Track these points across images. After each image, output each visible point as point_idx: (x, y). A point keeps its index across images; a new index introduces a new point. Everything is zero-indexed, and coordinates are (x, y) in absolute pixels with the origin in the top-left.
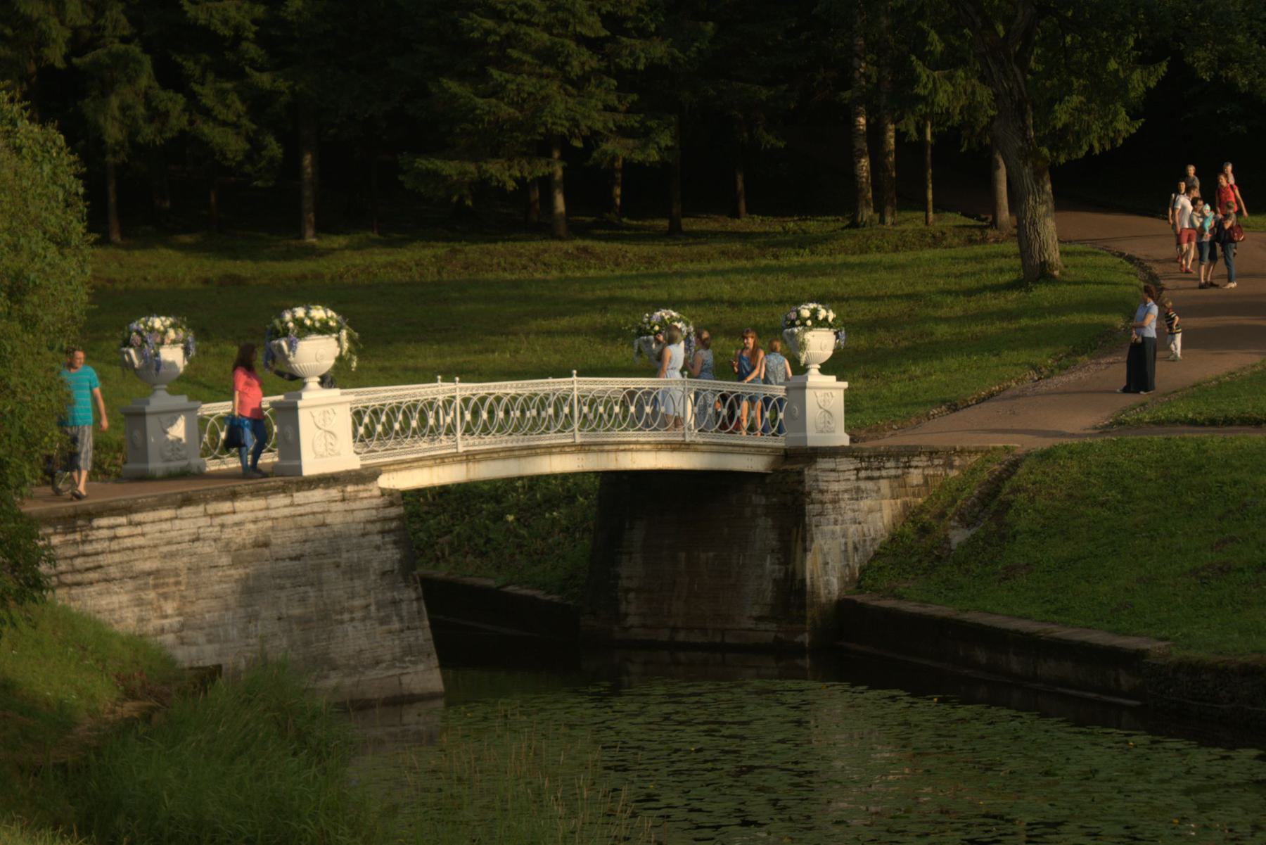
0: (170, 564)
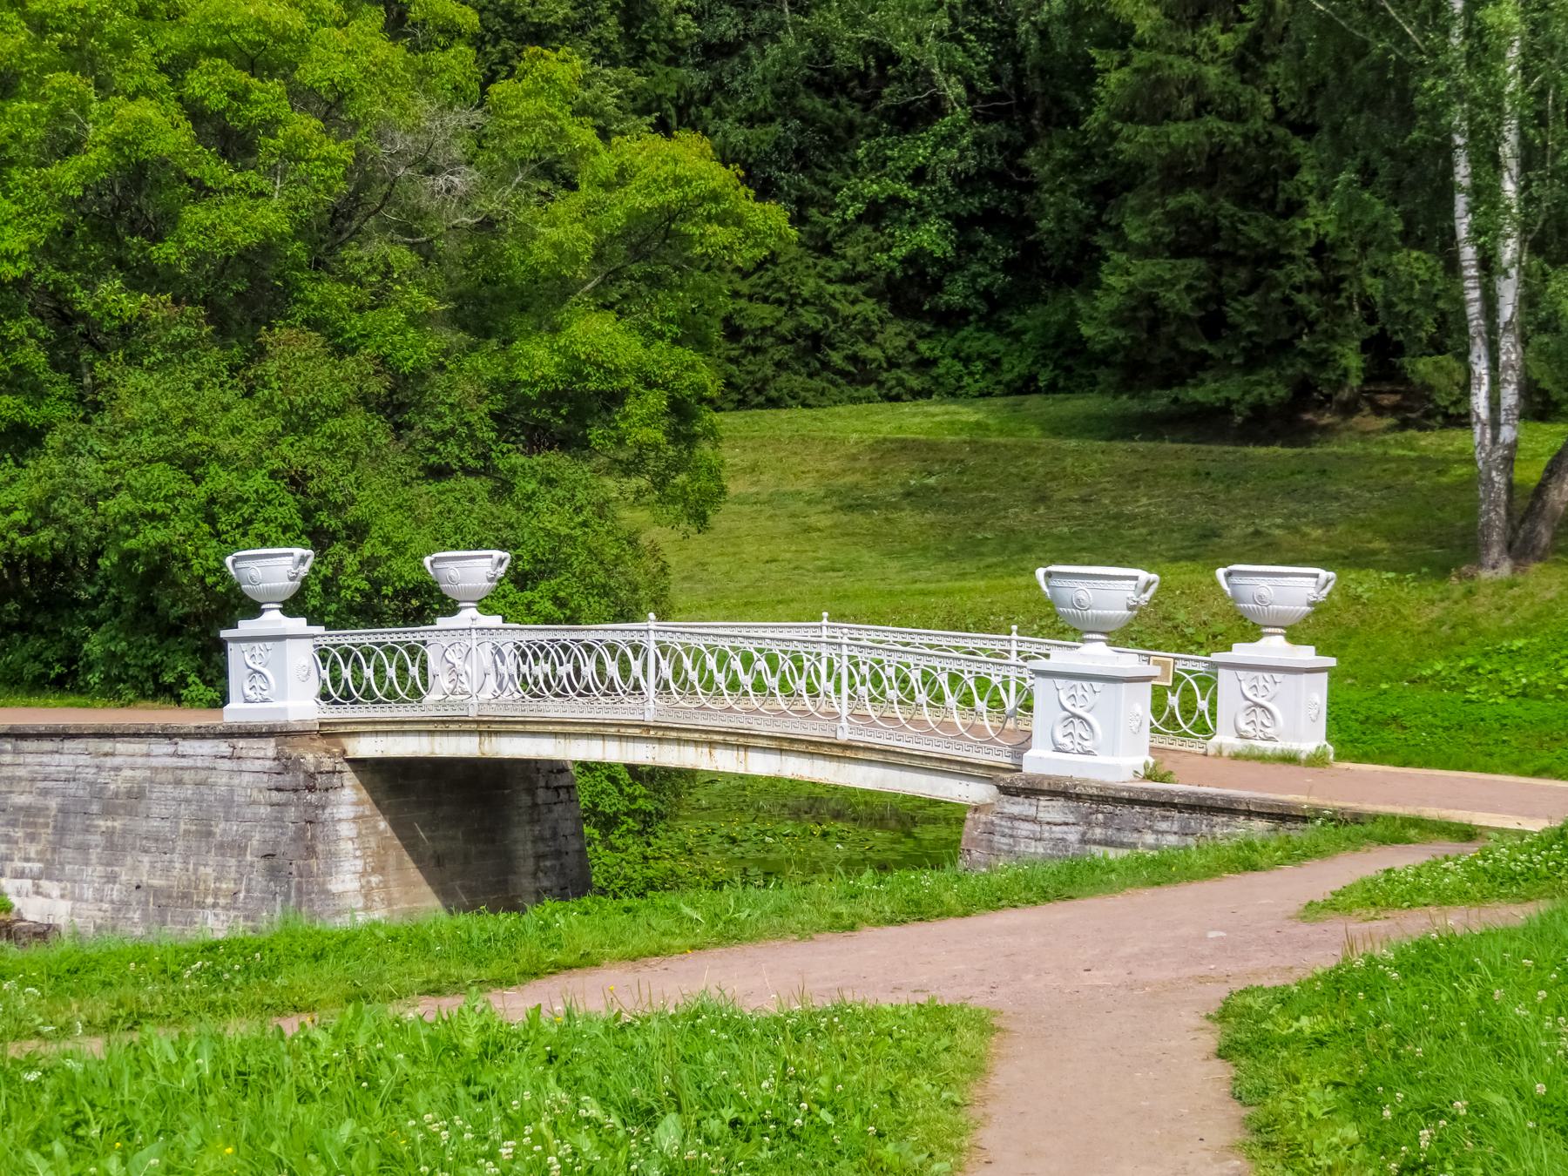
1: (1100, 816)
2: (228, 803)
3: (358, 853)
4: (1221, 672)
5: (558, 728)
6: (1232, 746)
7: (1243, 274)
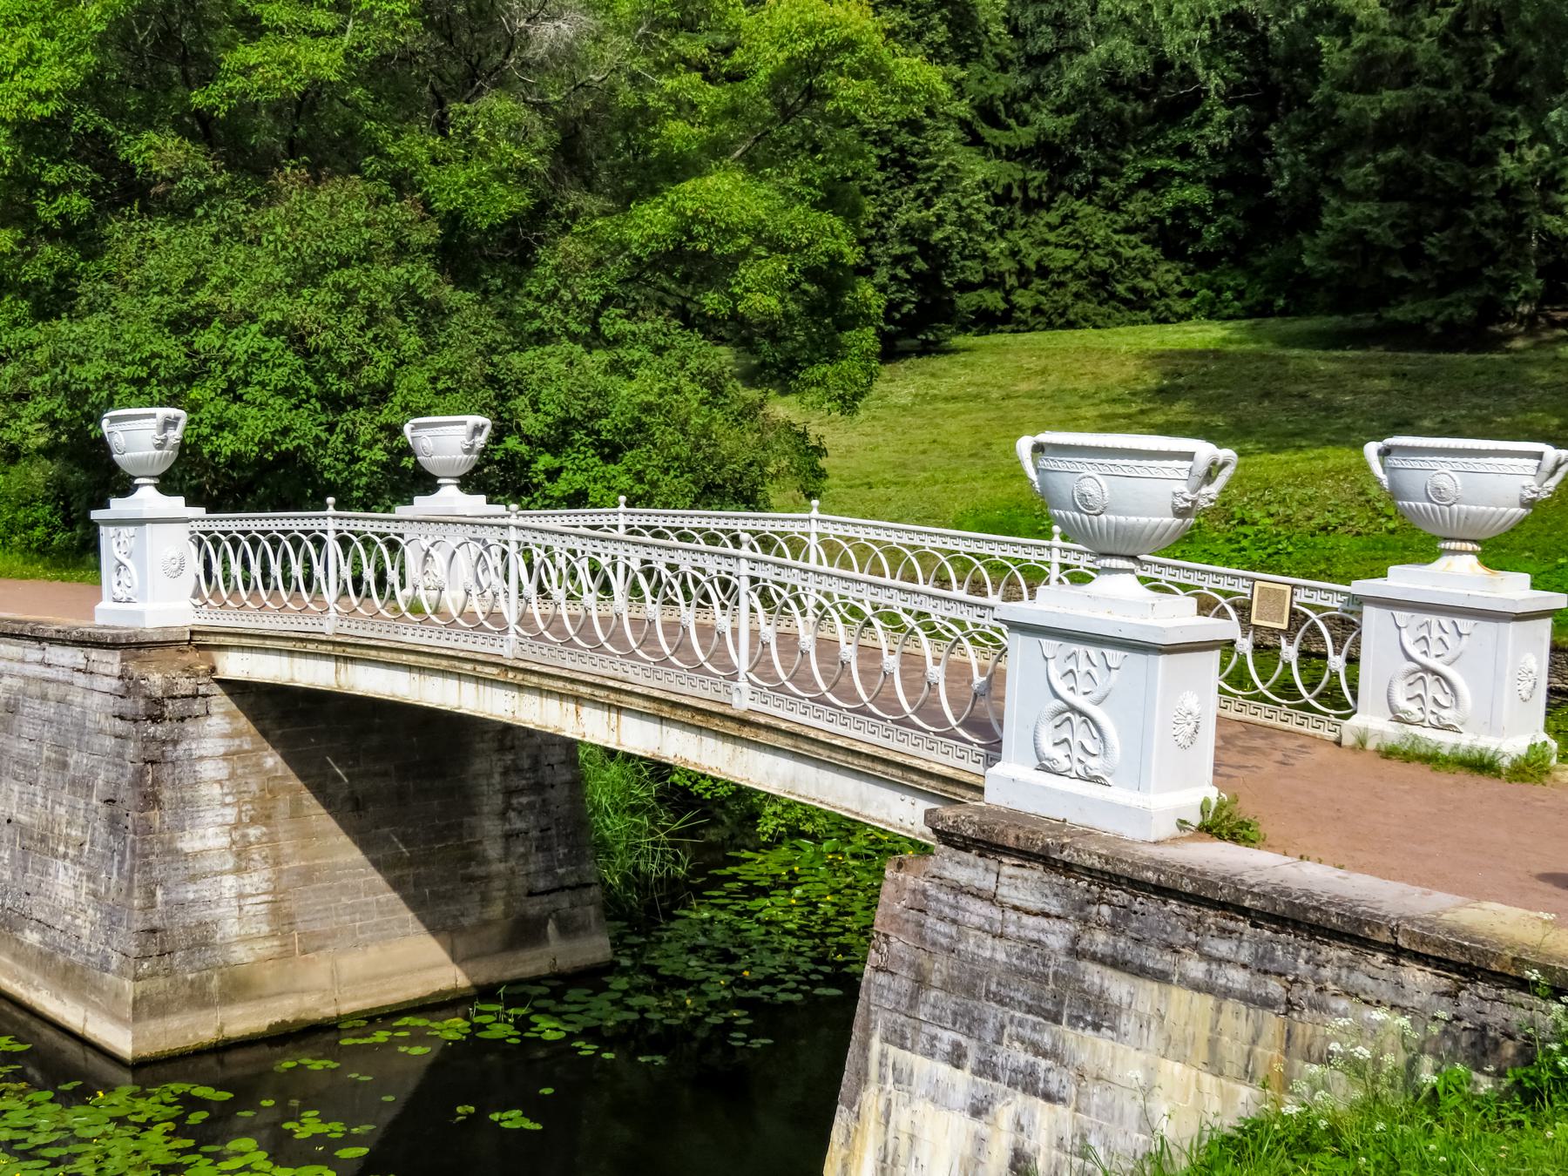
1: (1105, 910)
3: (229, 799)
4: (1369, 611)
5: (411, 659)
6: (1382, 734)
7: (1438, 213)
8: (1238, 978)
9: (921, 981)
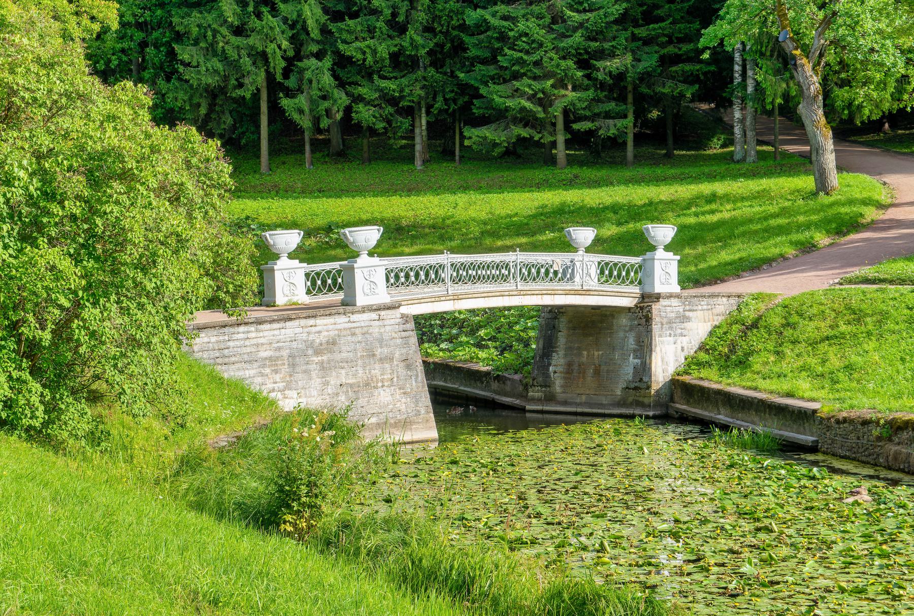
0: (277, 354)
2: (381, 341)
5: (485, 295)
8: (705, 307)
9: (662, 324)
